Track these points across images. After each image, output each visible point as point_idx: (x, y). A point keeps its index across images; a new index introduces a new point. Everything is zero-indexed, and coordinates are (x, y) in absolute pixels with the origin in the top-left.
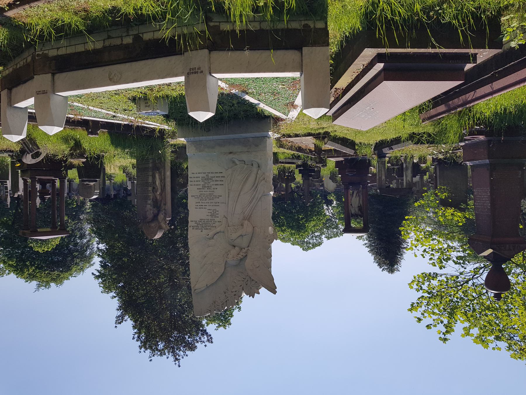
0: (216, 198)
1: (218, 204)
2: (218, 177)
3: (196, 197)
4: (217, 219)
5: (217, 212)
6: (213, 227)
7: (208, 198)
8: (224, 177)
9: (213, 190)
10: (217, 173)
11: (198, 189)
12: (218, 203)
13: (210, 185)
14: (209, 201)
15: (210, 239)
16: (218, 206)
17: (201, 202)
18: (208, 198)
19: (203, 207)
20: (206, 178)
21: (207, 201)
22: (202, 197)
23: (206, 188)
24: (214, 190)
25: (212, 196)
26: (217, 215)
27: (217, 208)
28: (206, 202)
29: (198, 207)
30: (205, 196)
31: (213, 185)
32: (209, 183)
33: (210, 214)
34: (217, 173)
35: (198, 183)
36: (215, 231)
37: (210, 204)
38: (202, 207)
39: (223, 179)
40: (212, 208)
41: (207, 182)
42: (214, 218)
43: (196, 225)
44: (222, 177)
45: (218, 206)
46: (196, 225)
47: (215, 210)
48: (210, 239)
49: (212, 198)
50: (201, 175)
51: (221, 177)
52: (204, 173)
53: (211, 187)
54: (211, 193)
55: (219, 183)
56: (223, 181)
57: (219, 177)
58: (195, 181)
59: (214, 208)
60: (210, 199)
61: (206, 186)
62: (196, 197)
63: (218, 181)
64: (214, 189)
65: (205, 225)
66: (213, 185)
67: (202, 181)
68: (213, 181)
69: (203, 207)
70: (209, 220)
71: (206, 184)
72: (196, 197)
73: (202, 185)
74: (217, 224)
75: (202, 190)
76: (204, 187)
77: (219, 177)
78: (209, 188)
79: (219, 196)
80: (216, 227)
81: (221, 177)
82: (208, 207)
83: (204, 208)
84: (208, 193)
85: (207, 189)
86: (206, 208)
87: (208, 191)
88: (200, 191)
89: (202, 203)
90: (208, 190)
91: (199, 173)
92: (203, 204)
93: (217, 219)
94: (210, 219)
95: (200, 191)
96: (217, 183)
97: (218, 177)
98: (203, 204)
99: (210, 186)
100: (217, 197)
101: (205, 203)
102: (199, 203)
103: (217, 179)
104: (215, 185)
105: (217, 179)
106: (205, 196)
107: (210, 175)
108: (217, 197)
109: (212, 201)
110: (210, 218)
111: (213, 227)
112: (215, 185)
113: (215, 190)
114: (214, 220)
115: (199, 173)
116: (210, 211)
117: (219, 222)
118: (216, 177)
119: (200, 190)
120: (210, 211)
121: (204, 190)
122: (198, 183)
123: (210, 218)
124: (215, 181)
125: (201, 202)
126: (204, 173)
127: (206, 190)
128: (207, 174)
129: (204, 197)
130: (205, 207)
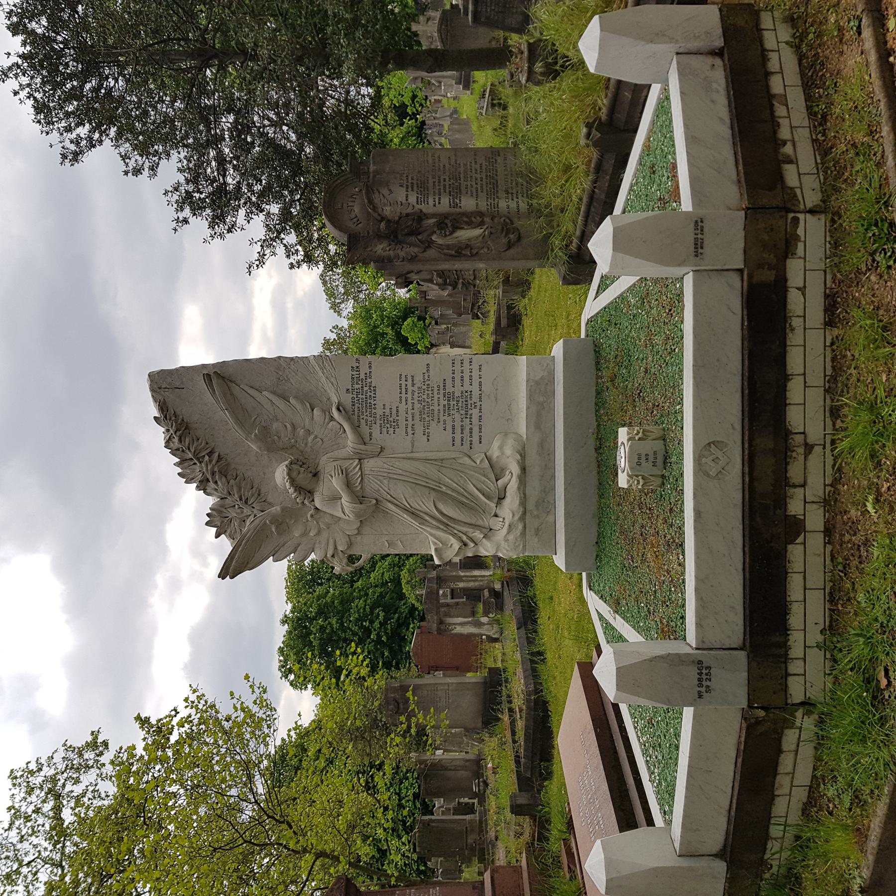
0: (424, 427)
2: (471, 432)
3: (426, 378)
4: (376, 429)
8: (471, 448)
10: (480, 429)
11: (445, 380)
12: (413, 434)
13: (452, 412)
14: (416, 411)
16: (407, 432)
17: (415, 388)
19: (404, 396)
20: (469, 402)
21: (417, 406)
23: (446, 402)
24: (442, 422)
25: (427, 419)
26: (384, 430)
33: (387, 412)
34: (480, 429)
35: (458, 382)
38: (404, 391)
40: (401, 419)
41: (460, 405)
42: (378, 422)
44: (471, 444)
45: (407, 432)
47: (398, 425)
49: (424, 418)
50: (475, 388)
51: (471, 441)
52: (480, 398)
54: (436, 412)
56: (462, 444)
57: (471, 437)
59: (402, 423)
60: (420, 412)
61: (452, 403)
62: (426, 375)
63: (462, 433)
64: (445, 421)
67: (462, 393)
69: (404, 396)
70: (374, 411)
71: (455, 403)
72: (426, 375)
73: (453, 392)
75: (442, 392)
76: (449, 396)
79: (428, 436)
81: (471, 441)
82: (402, 408)
83: (401, 397)
84: (436, 408)
85: (444, 406)
87: (439, 408)
88: (439, 386)
89: (413, 392)
90: (441, 407)
92: (409, 395)
96: (458, 430)
97: (471, 432)
99: (452, 412)
100: (427, 431)
102: (413, 385)
104: (453, 426)
107: (475, 413)
108: (427, 431)
109: (417, 417)
112: (453, 426)
114: (375, 423)
116: (394, 411)
117: (370, 435)
118: (471, 429)
119: (442, 387)
120: (394, 411)
121: (441, 396)
122: (458, 382)
123: (379, 411)
124: (462, 426)
125: (415, 388)
126: (480, 398)
128: (478, 404)
129: (425, 397)
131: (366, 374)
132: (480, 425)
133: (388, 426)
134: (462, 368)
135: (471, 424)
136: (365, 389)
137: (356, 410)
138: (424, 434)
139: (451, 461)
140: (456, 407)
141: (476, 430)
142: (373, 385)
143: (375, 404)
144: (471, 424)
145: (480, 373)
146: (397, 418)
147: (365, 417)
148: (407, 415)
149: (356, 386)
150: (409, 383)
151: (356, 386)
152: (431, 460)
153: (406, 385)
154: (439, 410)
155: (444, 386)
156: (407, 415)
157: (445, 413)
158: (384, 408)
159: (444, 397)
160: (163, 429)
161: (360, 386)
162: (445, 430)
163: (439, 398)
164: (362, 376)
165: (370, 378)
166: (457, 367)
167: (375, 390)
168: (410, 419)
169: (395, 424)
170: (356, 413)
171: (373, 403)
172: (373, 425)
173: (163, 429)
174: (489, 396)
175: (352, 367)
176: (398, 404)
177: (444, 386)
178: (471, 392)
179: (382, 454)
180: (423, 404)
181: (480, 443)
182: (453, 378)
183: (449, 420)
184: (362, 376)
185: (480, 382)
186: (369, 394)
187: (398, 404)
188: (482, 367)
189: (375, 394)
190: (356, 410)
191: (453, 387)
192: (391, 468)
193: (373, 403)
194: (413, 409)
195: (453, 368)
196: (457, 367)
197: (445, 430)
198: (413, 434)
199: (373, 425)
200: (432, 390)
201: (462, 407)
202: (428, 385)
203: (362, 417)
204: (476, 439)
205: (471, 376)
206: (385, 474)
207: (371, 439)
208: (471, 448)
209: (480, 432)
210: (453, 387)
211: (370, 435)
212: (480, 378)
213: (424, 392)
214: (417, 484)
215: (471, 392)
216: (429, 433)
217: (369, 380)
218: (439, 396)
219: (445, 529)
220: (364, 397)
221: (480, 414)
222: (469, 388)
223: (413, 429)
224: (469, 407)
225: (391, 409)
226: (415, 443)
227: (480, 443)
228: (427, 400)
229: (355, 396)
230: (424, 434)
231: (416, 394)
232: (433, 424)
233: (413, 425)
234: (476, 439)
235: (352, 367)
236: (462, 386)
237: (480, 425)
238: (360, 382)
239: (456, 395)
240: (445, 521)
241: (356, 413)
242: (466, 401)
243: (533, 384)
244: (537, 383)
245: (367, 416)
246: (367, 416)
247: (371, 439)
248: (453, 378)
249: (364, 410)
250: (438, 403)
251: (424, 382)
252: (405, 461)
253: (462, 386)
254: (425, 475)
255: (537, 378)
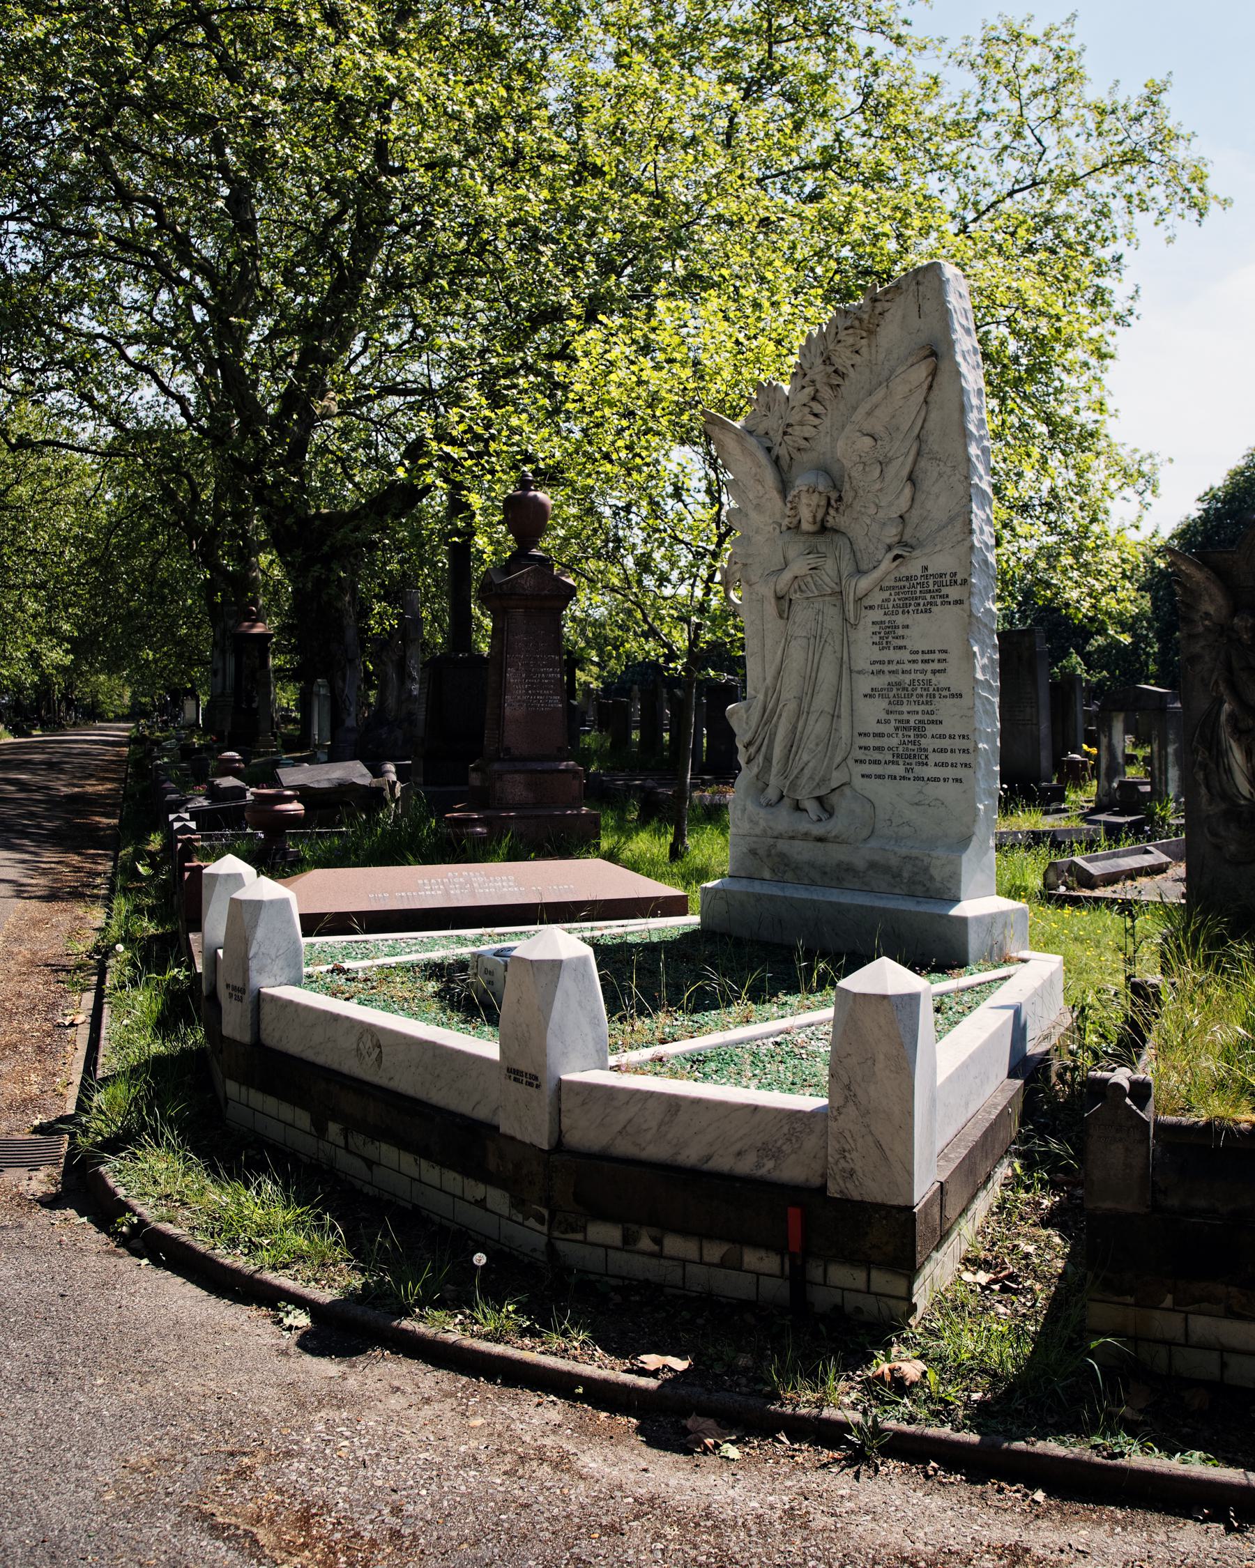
1: (877, 667)
3: (944, 693)
4: (877, 615)
5: (876, 639)
6: (889, 588)
9: (892, 717)
14: (901, 677)
17: (929, 676)
19: (919, 657)
26: (877, 629)
27: (877, 654)
28: (913, 676)
29: (937, 656)
33: (900, 632)
37: (900, 667)
38: (927, 657)
39: (860, 755)
40: (891, 654)
42: (887, 618)
43: (945, 591)
45: (874, 663)
46: (945, 591)
50: (931, 771)
54: (899, 708)
55: (871, 742)
61: (912, 733)
64: (887, 722)
66: (890, 735)
68: (890, 749)
69: (919, 657)
73: (925, 736)
74: (877, 598)
75: (926, 717)
76: (920, 728)
78: (903, 726)
82: (905, 655)
84: (905, 708)
88: (932, 713)
89: (924, 672)
90: (905, 717)
91: (936, 780)
92: (920, 666)
93: (877, 615)
95: (932, 713)
98: (920, 666)
102: (934, 672)
103: (877, 756)
105: (877, 756)
107: (899, 770)
109: (893, 679)
110: (900, 619)
111: (889, 588)
113: (883, 716)
115: (936, 780)
116: (900, 642)
119: (934, 717)
120: (900, 642)
121: (919, 717)
123: (900, 619)
125: (929, 676)
127: (912, 718)
128: (911, 775)
130: (914, 657)
150: (937, 666)
154: (901, 713)
166: (959, 744)
196: (959, 744)
222: (931, 762)
231: (921, 677)
232: (884, 704)
239: (923, 741)
250: (911, 711)
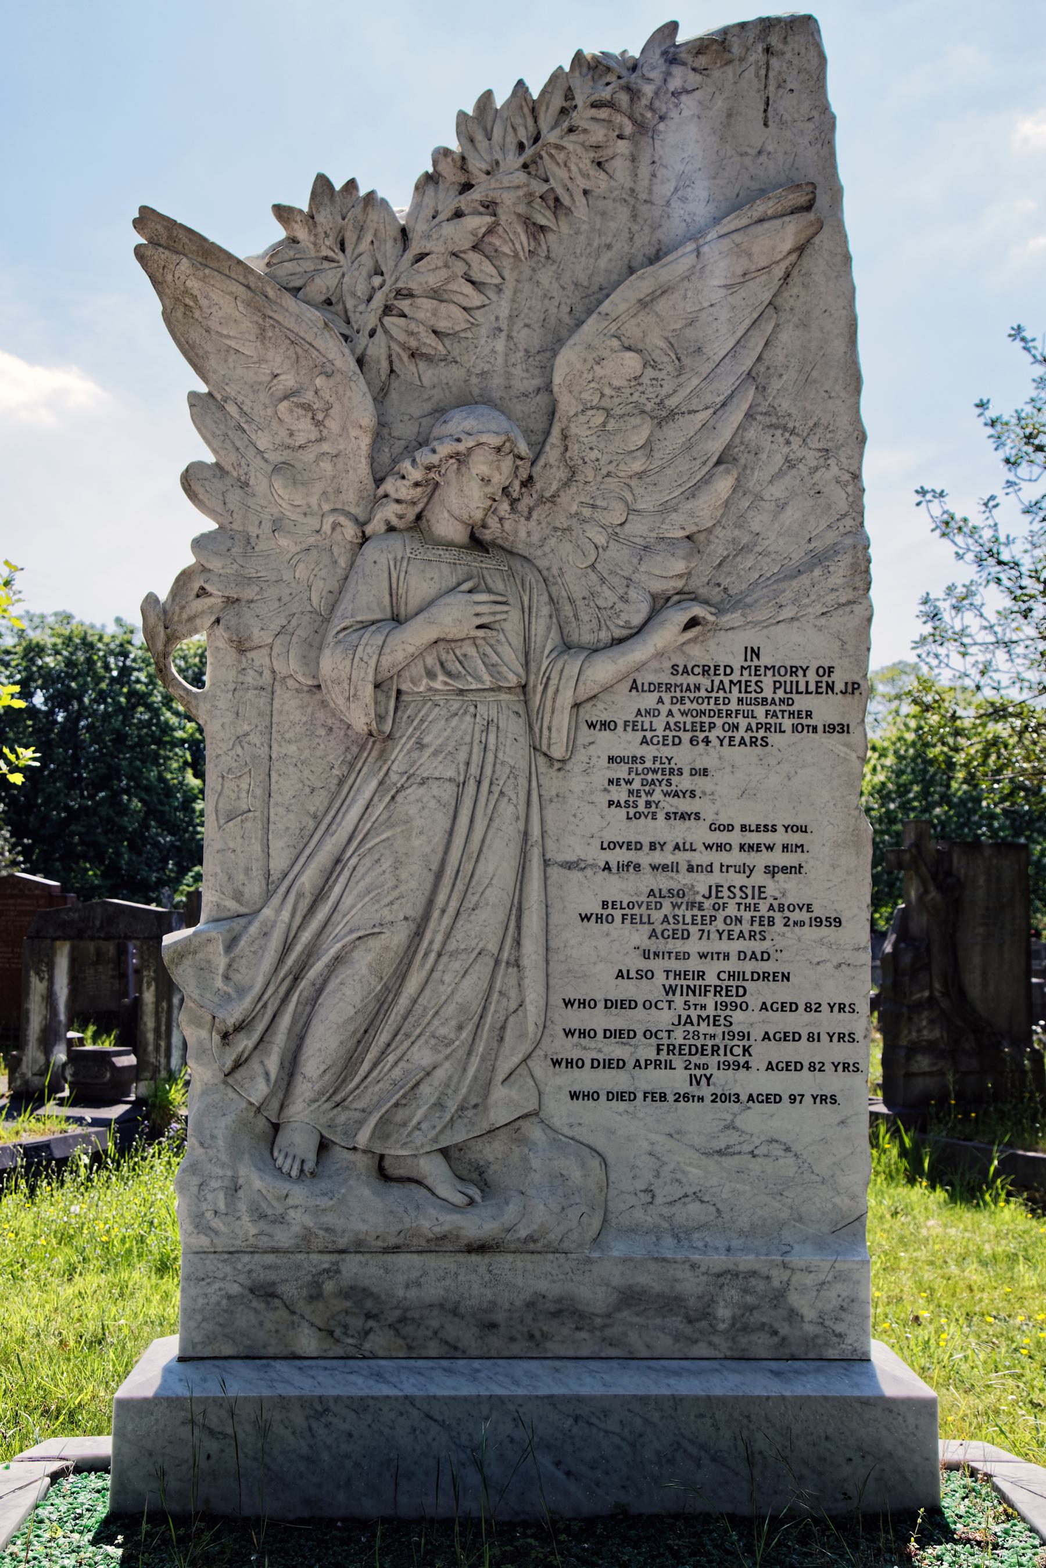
0: (631, 905)
2: (608, 1064)
7: (691, 905)
8: (556, 1063)
10: (620, 1096)
11: (786, 977)
12: (607, 867)
14: (684, 879)
15: (687, 596)
16: (612, 845)
18: (691, 905)
21: (701, 883)
22: (747, 915)
24: (644, 965)
27: (618, 826)
30: (719, 924)
31: (648, 1005)
32: (689, 1021)
34: (620, 1096)
36: (639, 652)
44: (570, 1063)
45: (612, 845)
48: (687, 596)
49: (659, 906)
51: (579, 1063)
52: (725, 1098)
53: (670, 990)
56: (569, 1033)
57: (595, 1064)
58: (811, 1037)
60: (681, 893)
62: (804, 916)
63: (608, 1034)
65: (727, 701)
72: (804, 916)
77: (595, 1064)
79: (599, 918)
80: (634, 686)
81: (579, 1063)
86: (714, 827)
87: (695, 958)
88: (765, 956)
94: (677, 742)
95: (765, 956)
96: (617, 1020)
97: (608, 1064)
101: (725, 868)
106: (719, 924)
108: (618, 914)
109: (664, 882)
114: (644, 741)
117: (605, 725)
124: (631, 1034)
126: (725, 1098)
129: (732, 910)
131: (809, 714)
132: (632, 1096)
133: (636, 785)
134: (825, 1038)
135: (637, 1064)
136: (760, 711)
137: (692, 680)
138: (605, 905)
139: (513, 993)
140: (694, 1014)
141: (618, 1080)
142: (774, 738)
143: (707, 741)
144: (637, 1064)
145: (808, 1099)
146: (661, 816)
147: (664, 709)
148: (669, 847)
149: (768, 681)
151: (768, 681)
152: (519, 927)
153: (770, 848)
155: (765, 976)
156: (669, 847)
157: (677, 975)
158: (694, 772)
159: (731, 975)
160: (635, 52)
161: (768, 693)
162: (620, 975)
163: (727, 956)
164: (802, 703)
165: (794, 728)
167: (753, 742)
168: (659, 857)
169: (641, 807)
170: (679, 679)
171: (712, 736)
172: (640, 735)
173: (635, 52)
174: (731, 1126)
175: (830, 670)
176: (708, 816)
177: (765, 976)
178: (747, 1066)
179: (541, 760)
180: (707, 904)
181: (574, 1096)
182: (794, 1007)
183: (653, 990)
184: (802, 703)
185: (777, 1099)
186: (743, 723)
187: (708, 816)
188: (826, 1109)
189: (742, 742)
190: (692, 680)
191: (764, 1007)
192: (496, 790)
193: (712, 736)
194: (690, 869)
195: (825, 1008)
197: (620, 975)
198: (607, 867)
199: (640, 735)
200: (752, 935)
201: (696, 1035)
202: (771, 922)
203: (666, 697)
204: (586, 1079)
205: (798, 1066)
206: (474, 770)
207: (592, 725)
208: (556, 1063)
209: (612, 1096)
210: (764, 1007)
211: (605, 725)
212: (793, 1099)
213: (747, 907)
214: (439, 875)
215: (747, 1066)
216: (610, 920)
217: (787, 723)
218: (734, 957)
219: (282, 973)
220: (733, 706)
221: (671, 1098)
223: (624, 867)
224: (695, 1059)
225: (693, 794)
226: (575, 875)
227: (574, 1096)
228: (721, 915)
229: (735, 677)
230: (605, 905)
233: (637, 867)
234: (586, 1079)
235: (830, 670)
236: (766, 1037)
237: (632, 1096)
238: (780, 693)
240: (312, 974)
241: (679, 679)
242: (715, 1050)
243: (776, 1283)
244: (778, 1297)
245: (670, 713)
246: (670, 713)
247: (592, 725)
248: (794, 1007)
249: (688, 706)
251: (781, 908)
252: (519, 839)
253: (766, 1037)
254: (467, 905)
255: (795, 1300)
